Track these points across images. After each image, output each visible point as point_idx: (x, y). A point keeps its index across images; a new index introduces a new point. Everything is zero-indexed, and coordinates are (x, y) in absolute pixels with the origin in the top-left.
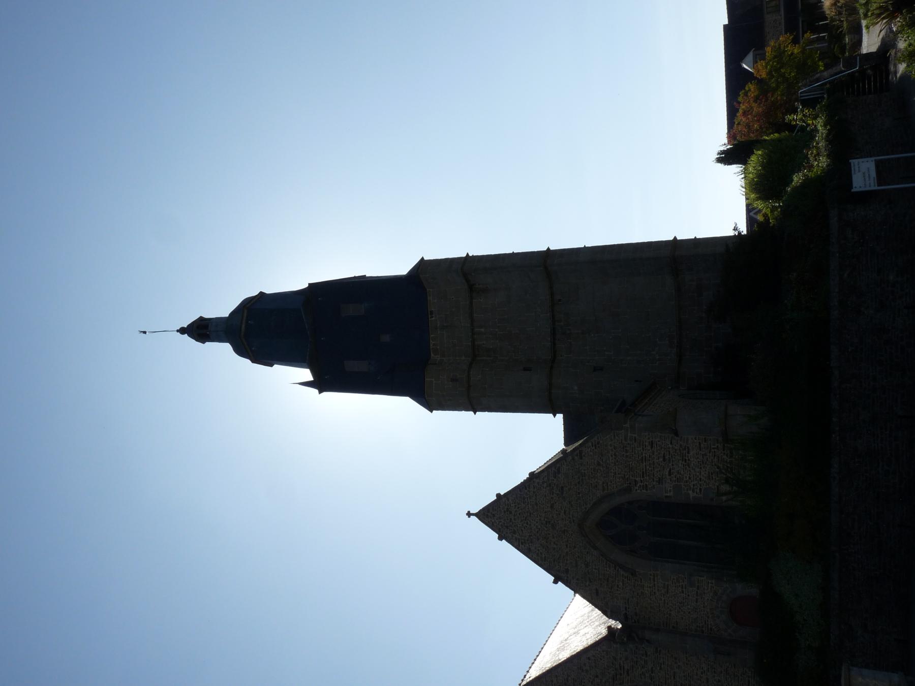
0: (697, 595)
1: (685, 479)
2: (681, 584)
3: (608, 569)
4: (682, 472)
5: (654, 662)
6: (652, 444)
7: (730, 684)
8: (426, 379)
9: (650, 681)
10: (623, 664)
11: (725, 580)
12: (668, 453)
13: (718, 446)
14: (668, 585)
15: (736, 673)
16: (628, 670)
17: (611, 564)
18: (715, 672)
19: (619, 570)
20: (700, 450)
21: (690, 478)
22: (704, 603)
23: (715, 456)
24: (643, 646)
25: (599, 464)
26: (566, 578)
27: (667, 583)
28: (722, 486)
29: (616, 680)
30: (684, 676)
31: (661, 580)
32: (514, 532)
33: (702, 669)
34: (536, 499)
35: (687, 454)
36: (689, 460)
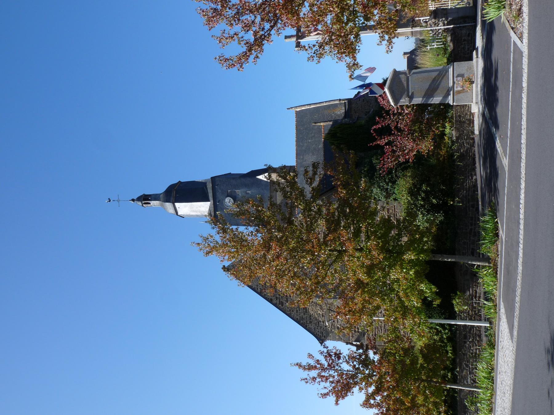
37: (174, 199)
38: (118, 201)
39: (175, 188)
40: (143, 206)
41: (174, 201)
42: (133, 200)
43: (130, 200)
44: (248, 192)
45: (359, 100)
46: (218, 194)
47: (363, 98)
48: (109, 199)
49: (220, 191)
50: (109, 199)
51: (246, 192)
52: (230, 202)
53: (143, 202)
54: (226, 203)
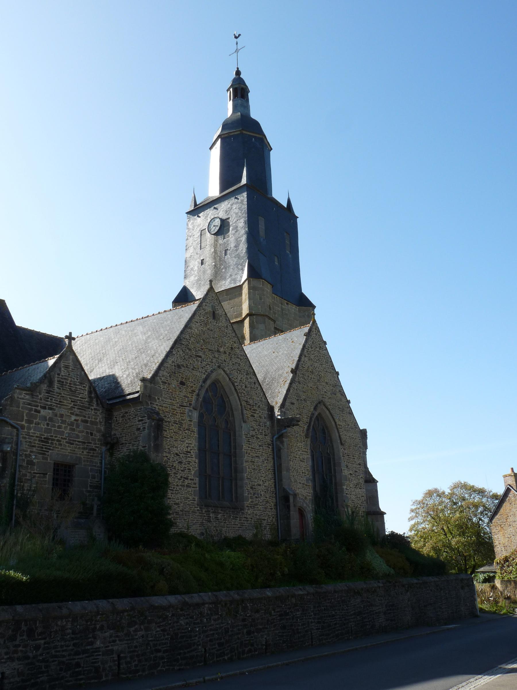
0: (303, 484)
1: (350, 484)
2: (306, 472)
3: (306, 417)
4: (352, 483)
5: (262, 441)
6: (360, 464)
7: (261, 504)
8: (269, 285)
9: (251, 434)
10: (258, 414)
11: (313, 506)
12: (358, 474)
13: (364, 508)
14: (305, 462)
15: (267, 509)
16: (254, 416)
17: (308, 420)
18: (265, 492)
19: (307, 426)
20: (362, 496)
21: (351, 487)
22: (300, 489)
23: (360, 505)
24: (270, 434)
25: (348, 425)
26: (296, 380)
27: (305, 461)
28: (350, 508)
29: (246, 403)
30: (259, 465)
31: (306, 457)
32: (312, 348)
33: (265, 482)
34: (328, 372)
35: (359, 487)
36: (357, 488)
37: (226, 135)
38: (237, 51)
39: (244, 132)
40: (227, 91)
41: (223, 136)
42: (238, 73)
43: (238, 68)
44: (228, 252)
45: (139, 421)
46: (226, 202)
47: (142, 428)
48: (239, 35)
49: (229, 206)
50: (239, 35)
51: (228, 249)
52: (214, 227)
53: (231, 90)
54: (213, 221)
